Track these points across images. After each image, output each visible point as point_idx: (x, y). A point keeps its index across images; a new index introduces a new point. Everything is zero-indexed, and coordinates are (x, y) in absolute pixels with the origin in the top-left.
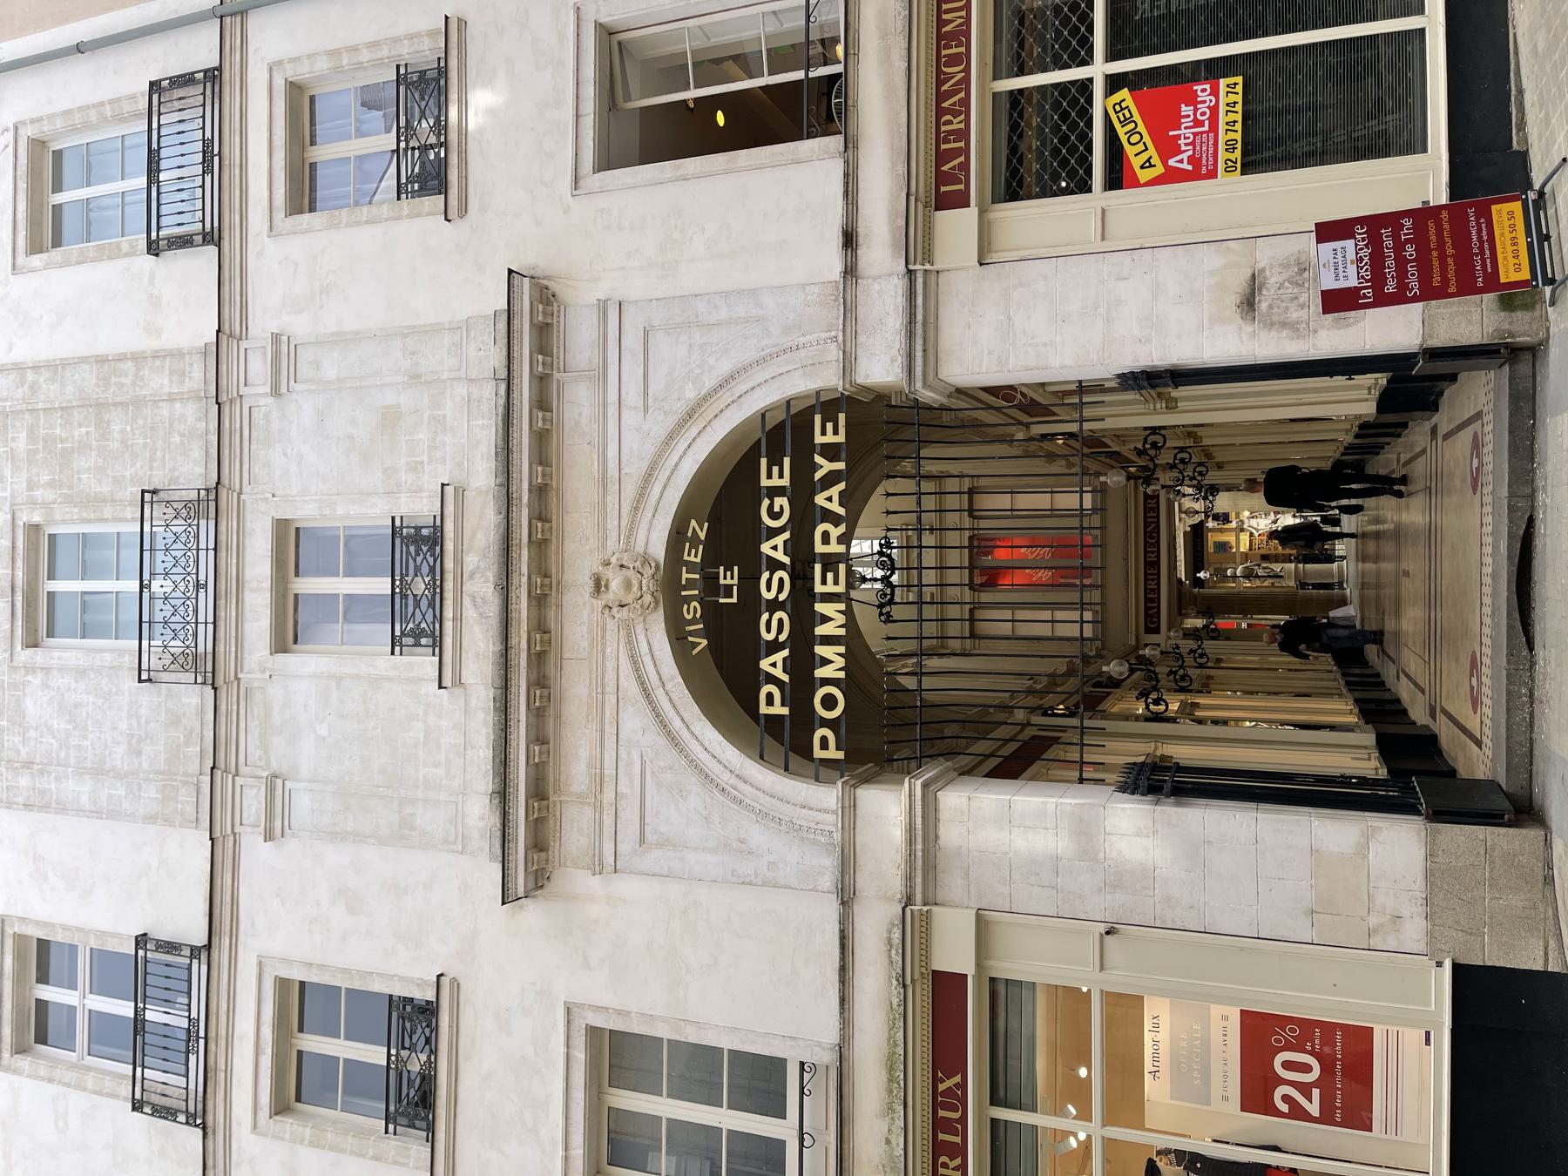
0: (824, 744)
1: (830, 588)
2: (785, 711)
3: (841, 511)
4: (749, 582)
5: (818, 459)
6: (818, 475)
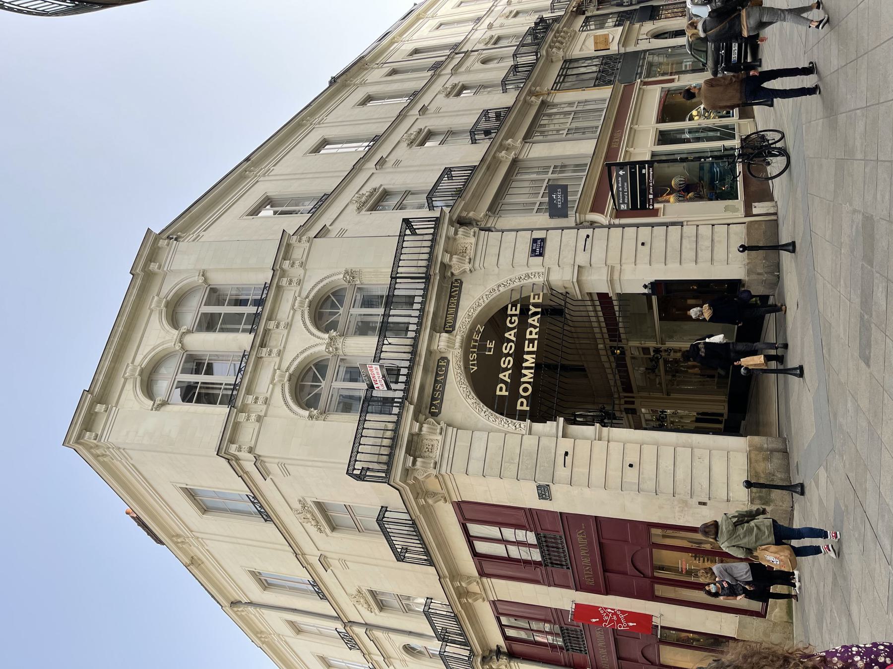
1: (531, 349)
2: (507, 394)
3: (538, 325)
4: (498, 348)
5: (531, 307)
6: (530, 313)
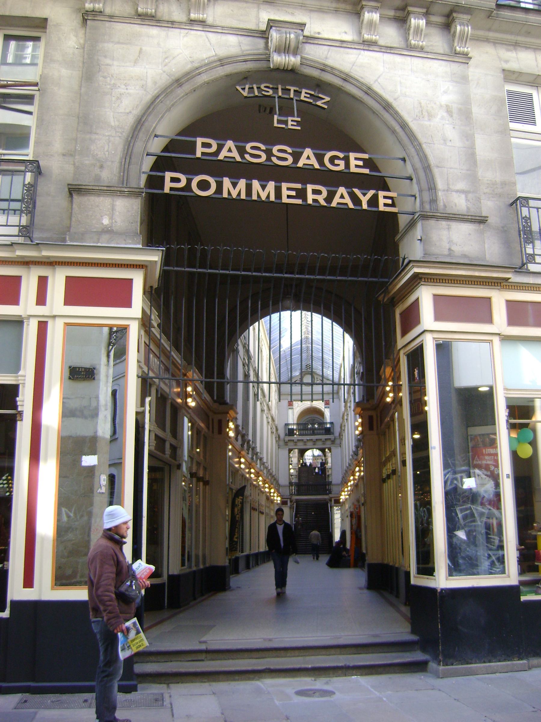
1: (285, 193)
3: (334, 204)
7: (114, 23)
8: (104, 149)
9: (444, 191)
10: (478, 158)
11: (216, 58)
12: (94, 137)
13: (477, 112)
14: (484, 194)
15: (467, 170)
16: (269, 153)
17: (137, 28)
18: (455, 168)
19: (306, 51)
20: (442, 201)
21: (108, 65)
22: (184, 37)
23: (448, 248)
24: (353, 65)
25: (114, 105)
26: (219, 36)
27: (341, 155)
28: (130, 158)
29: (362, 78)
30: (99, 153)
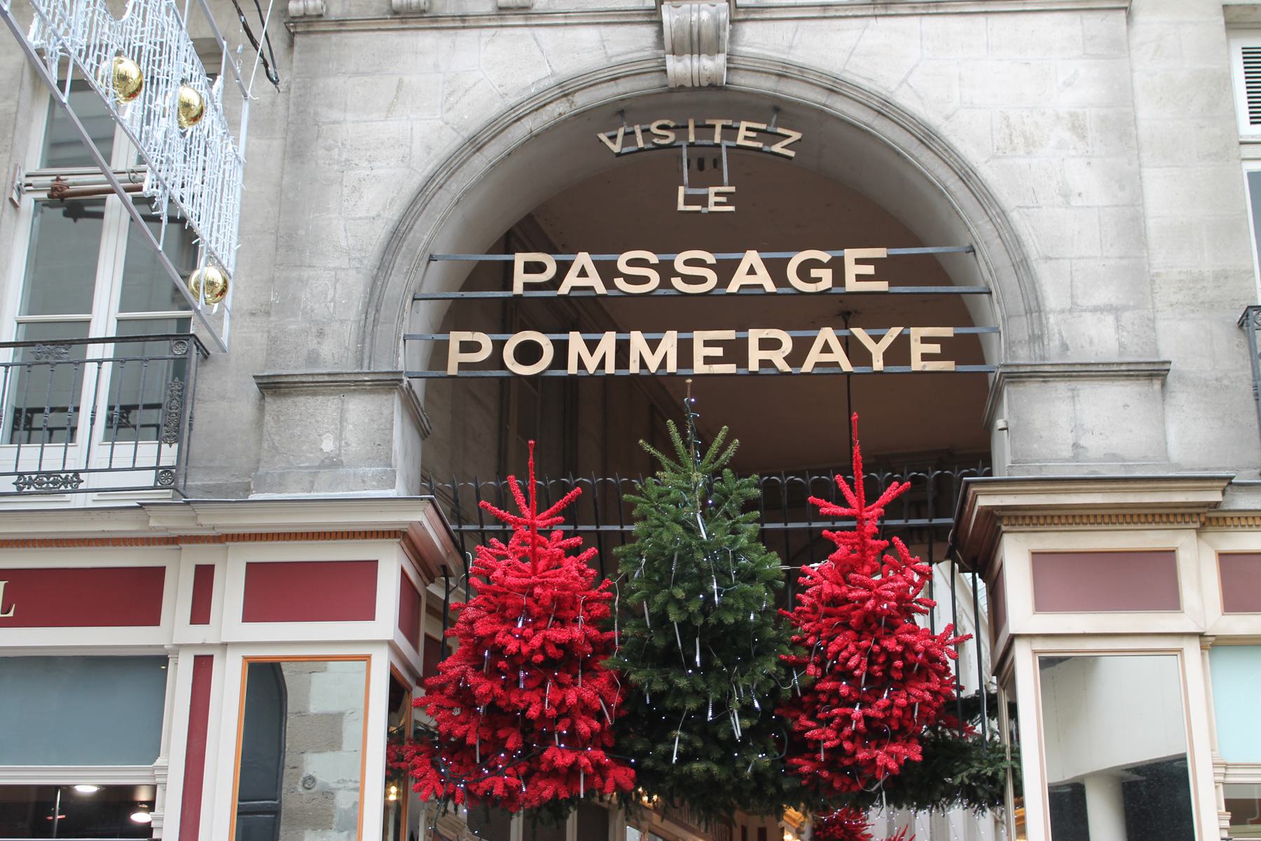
0: (468, 347)
1: (700, 352)
3: (807, 367)
7: (348, 34)
8: (325, 298)
9: (1062, 311)
10: (1151, 223)
11: (552, 81)
12: (306, 273)
13: (1148, 114)
14: (1172, 305)
15: (1121, 258)
16: (666, 270)
17: (393, 39)
18: (1090, 257)
19: (745, 39)
20: (1057, 336)
21: (334, 122)
22: (486, 44)
23: (1071, 442)
24: (851, 54)
25: (346, 204)
26: (560, 32)
27: (825, 257)
28: (377, 311)
29: (870, 80)
30: (316, 306)
